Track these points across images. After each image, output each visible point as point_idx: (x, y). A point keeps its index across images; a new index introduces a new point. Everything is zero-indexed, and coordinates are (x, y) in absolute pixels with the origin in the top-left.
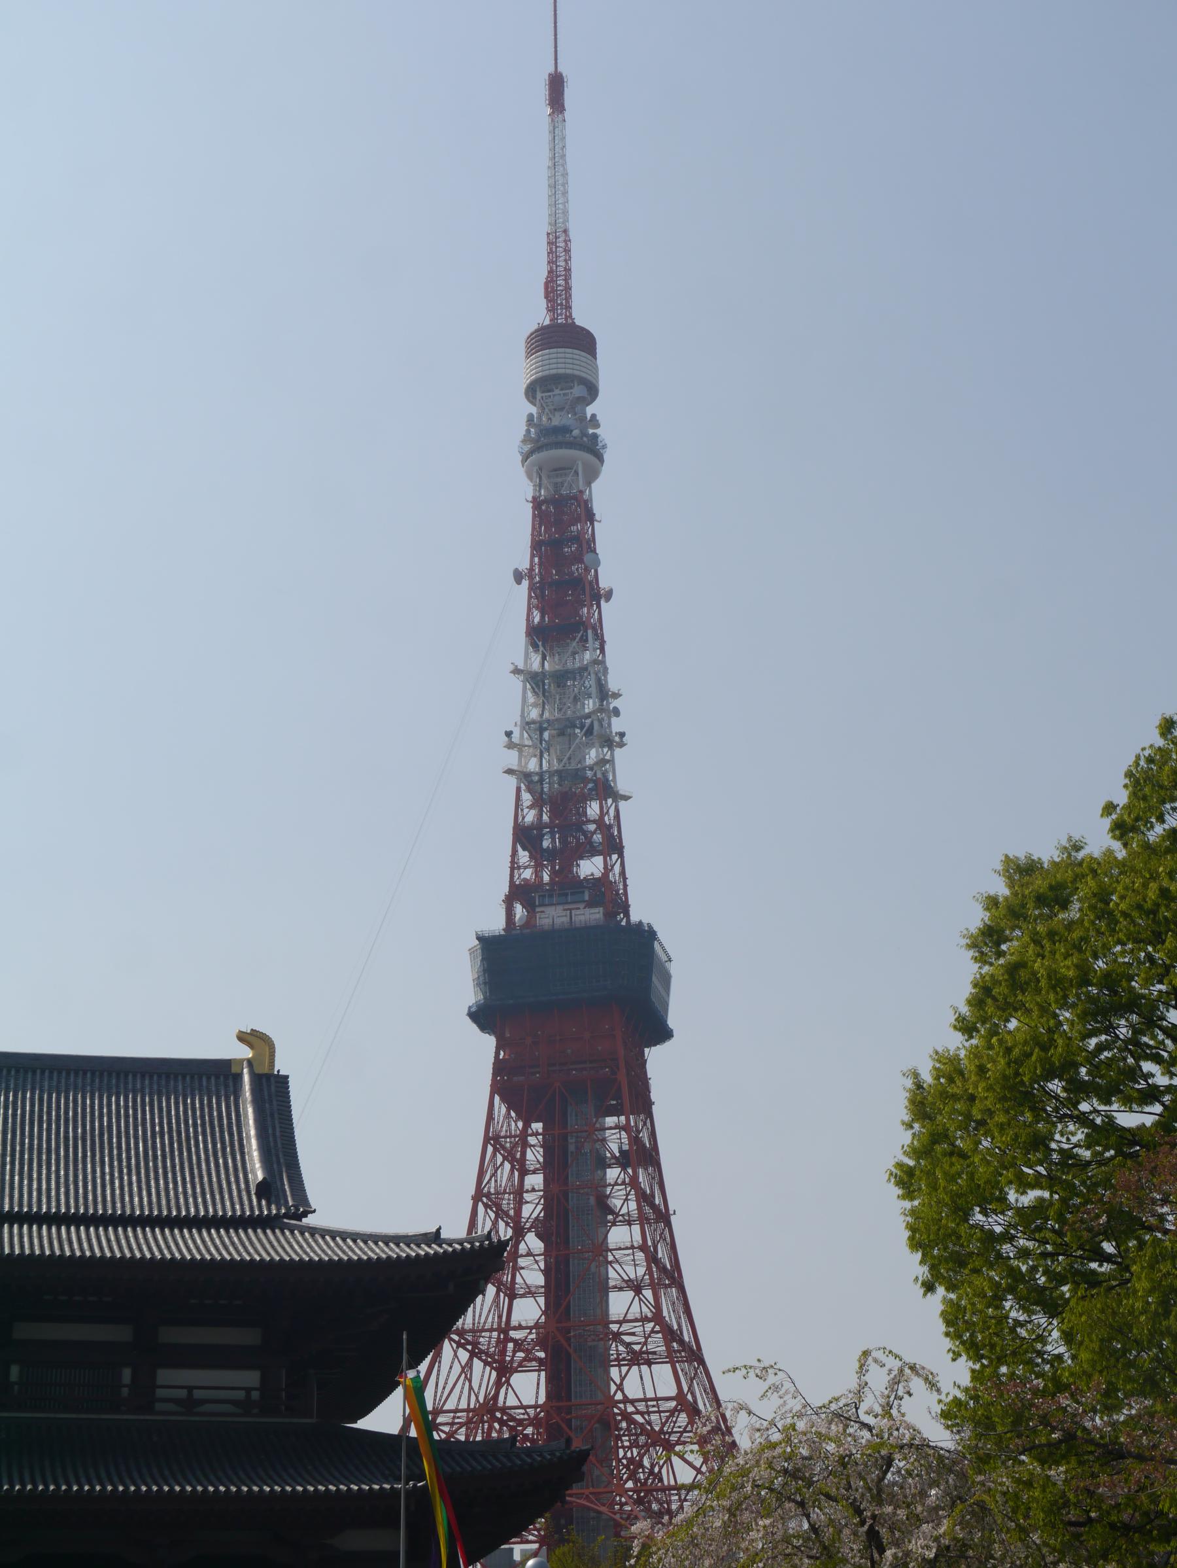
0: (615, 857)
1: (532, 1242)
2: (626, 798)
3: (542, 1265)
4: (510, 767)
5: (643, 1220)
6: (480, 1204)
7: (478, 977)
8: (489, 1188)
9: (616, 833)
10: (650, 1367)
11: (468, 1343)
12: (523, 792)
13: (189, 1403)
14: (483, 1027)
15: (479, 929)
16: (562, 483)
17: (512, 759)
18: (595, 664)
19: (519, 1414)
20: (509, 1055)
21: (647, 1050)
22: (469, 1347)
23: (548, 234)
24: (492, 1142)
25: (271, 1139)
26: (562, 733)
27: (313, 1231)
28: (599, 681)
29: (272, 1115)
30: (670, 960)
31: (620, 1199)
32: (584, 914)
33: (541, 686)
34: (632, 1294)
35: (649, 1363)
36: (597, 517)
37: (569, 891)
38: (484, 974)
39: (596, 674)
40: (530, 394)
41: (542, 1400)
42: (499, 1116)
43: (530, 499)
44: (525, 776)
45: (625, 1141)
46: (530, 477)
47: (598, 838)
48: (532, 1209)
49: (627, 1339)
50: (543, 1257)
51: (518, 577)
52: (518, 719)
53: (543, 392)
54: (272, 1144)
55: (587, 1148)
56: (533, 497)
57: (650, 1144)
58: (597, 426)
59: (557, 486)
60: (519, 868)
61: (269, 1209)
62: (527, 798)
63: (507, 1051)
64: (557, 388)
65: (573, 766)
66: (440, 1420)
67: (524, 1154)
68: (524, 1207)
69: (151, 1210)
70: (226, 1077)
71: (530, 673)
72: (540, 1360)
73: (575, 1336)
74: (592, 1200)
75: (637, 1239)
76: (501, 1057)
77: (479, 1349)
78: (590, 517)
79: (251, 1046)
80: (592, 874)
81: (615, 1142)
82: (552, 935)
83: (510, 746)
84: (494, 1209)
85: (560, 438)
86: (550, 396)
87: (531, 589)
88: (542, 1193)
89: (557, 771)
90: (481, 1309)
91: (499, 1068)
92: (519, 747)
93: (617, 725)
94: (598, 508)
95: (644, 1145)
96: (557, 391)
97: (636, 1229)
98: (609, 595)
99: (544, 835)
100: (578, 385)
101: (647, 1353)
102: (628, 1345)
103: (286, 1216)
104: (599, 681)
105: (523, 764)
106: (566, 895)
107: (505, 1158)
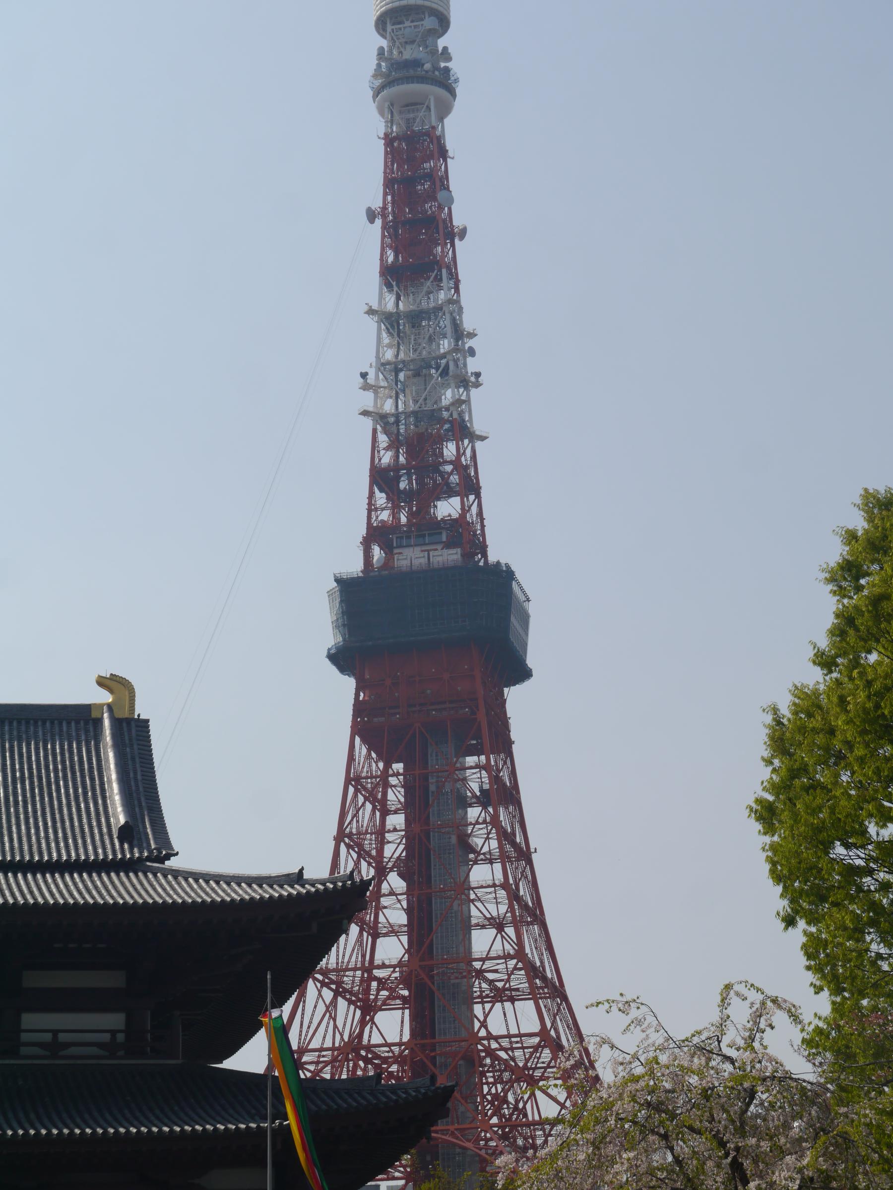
0: (472, 497)
1: (395, 881)
2: (483, 438)
3: (405, 904)
4: (366, 408)
5: (504, 858)
6: (342, 844)
7: (337, 619)
8: (351, 828)
9: (473, 474)
10: (513, 1003)
11: (332, 982)
12: (379, 433)
13: (55, 1047)
14: (343, 669)
15: (337, 572)
16: (414, 119)
17: (367, 400)
18: (449, 304)
19: (384, 1052)
20: (370, 697)
21: (506, 690)
22: (333, 987)
24: (353, 783)
25: (133, 783)
26: (417, 374)
27: (176, 874)
28: (454, 320)
29: (133, 759)
30: (528, 600)
31: (482, 838)
32: (441, 555)
33: (396, 327)
34: (494, 931)
35: (512, 1000)
36: (450, 154)
37: (427, 533)
38: (343, 616)
39: (451, 314)
40: (380, 26)
41: (406, 1037)
42: (360, 757)
43: (382, 136)
44: (381, 418)
45: (486, 780)
46: (382, 113)
47: (454, 479)
48: (393, 849)
49: (490, 976)
50: (405, 896)
51: (371, 216)
52: (373, 360)
53: (394, 24)
54: (134, 788)
55: (448, 788)
56: (386, 135)
57: (510, 783)
58: (449, 59)
59: (409, 123)
60: (376, 509)
61: (132, 852)
62: (383, 439)
63: (367, 692)
64: (407, 20)
65: (429, 407)
66: (305, 1059)
67: (385, 794)
68: (386, 847)
69: (13, 855)
70: (87, 722)
71: (384, 313)
72: (403, 998)
73: (438, 974)
74: (454, 839)
75: (499, 877)
76: (361, 698)
77: (344, 988)
78: (443, 153)
79: (111, 691)
80: (450, 515)
81: (476, 782)
82: (412, 576)
83: (366, 387)
84: (356, 849)
85: (412, 72)
86: (400, 29)
87: (384, 227)
88: (403, 833)
89: (413, 412)
90: (345, 948)
91: (359, 709)
92: (375, 389)
93: (473, 365)
94: (450, 144)
95: (505, 784)
96: (407, 24)
97: (498, 867)
98: (463, 233)
99: (401, 476)
100: (429, 16)
101: (510, 989)
102: (491, 982)
103: (149, 859)
104: (454, 320)
105: (379, 406)
106: (424, 536)
107: (366, 799)
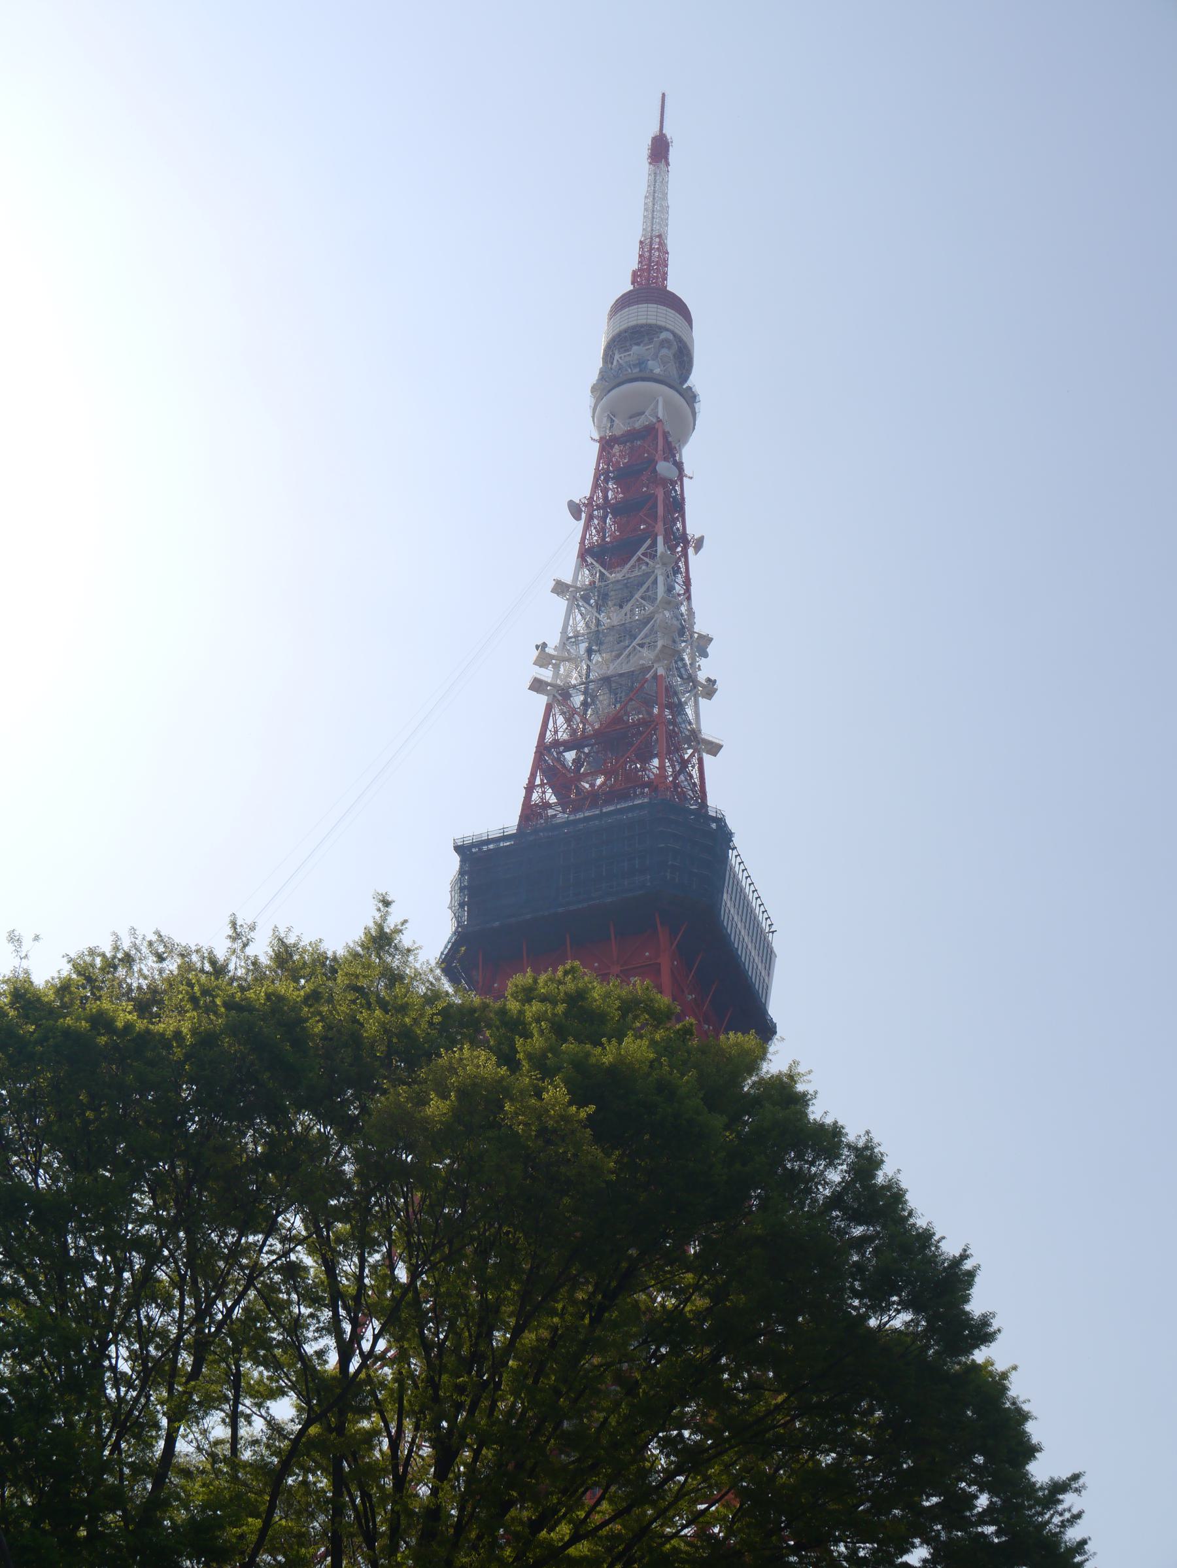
2: (714, 749)
15: (458, 836)
23: (641, 242)
43: (597, 438)
44: (559, 696)
51: (575, 510)
